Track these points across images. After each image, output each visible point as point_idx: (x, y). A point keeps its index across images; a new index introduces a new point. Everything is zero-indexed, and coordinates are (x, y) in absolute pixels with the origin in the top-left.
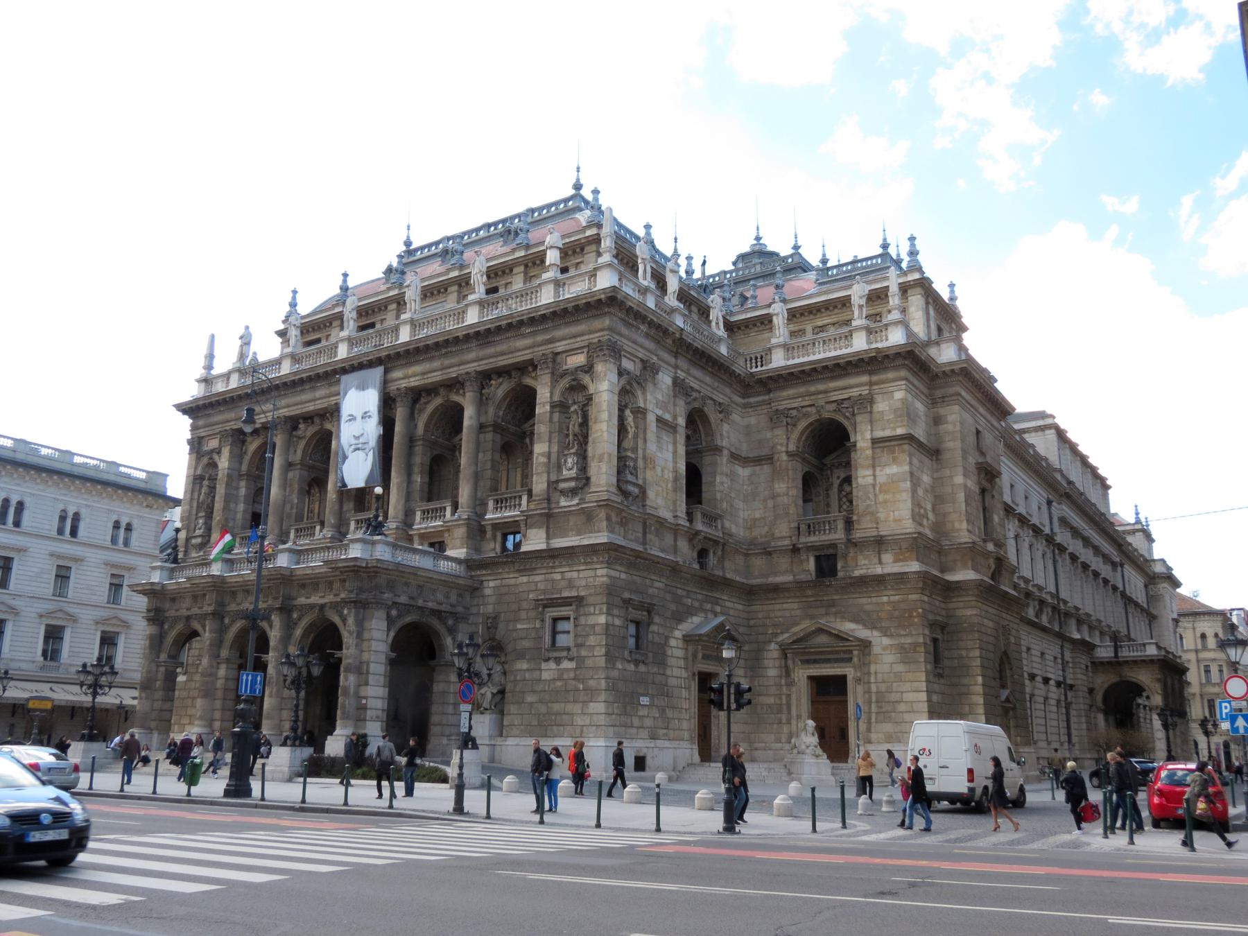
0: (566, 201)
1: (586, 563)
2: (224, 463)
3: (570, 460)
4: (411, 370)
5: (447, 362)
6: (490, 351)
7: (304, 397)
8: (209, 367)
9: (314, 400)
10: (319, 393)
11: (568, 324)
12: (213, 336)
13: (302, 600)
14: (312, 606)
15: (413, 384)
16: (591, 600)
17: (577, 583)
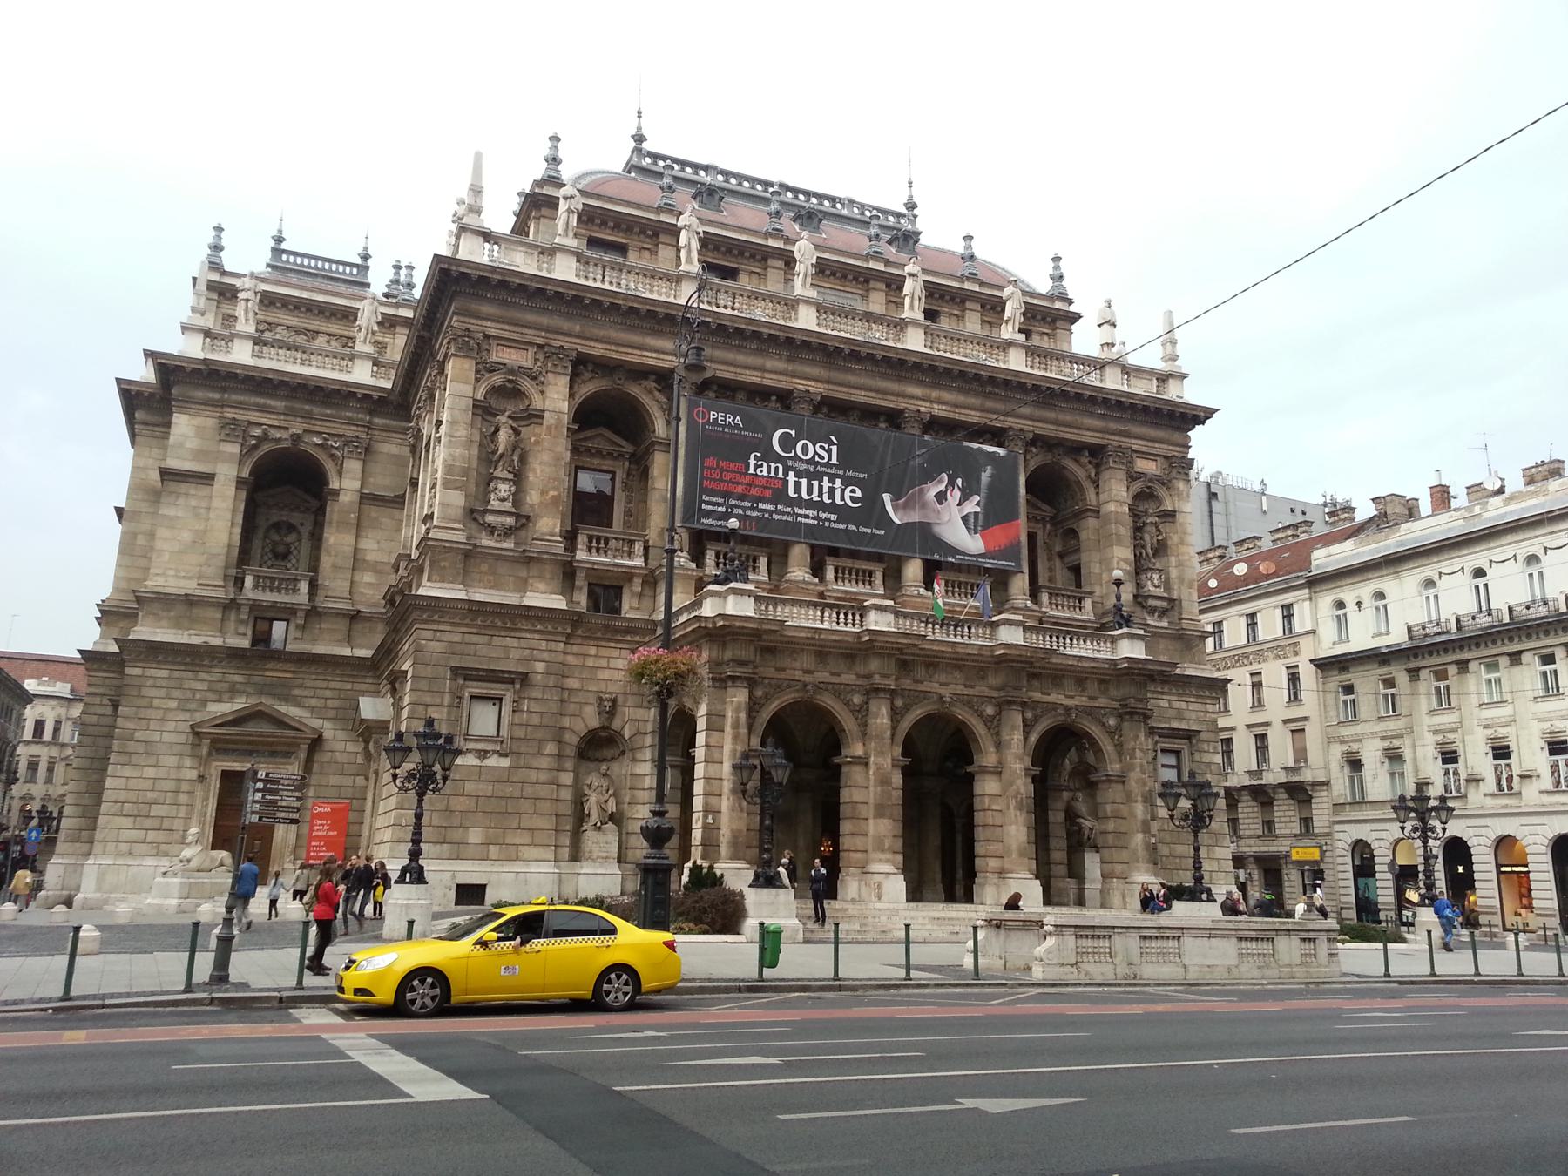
0: (899, 215)
1: (1198, 696)
2: (556, 399)
3: (1156, 576)
4: (935, 394)
5: (989, 404)
6: (1051, 415)
7: (741, 358)
8: (476, 210)
9: (763, 370)
10: (769, 364)
11: (1144, 423)
12: (478, 157)
13: (1037, 696)
14: (1053, 706)
15: (936, 412)
16: (1203, 736)
17: (1187, 715)
